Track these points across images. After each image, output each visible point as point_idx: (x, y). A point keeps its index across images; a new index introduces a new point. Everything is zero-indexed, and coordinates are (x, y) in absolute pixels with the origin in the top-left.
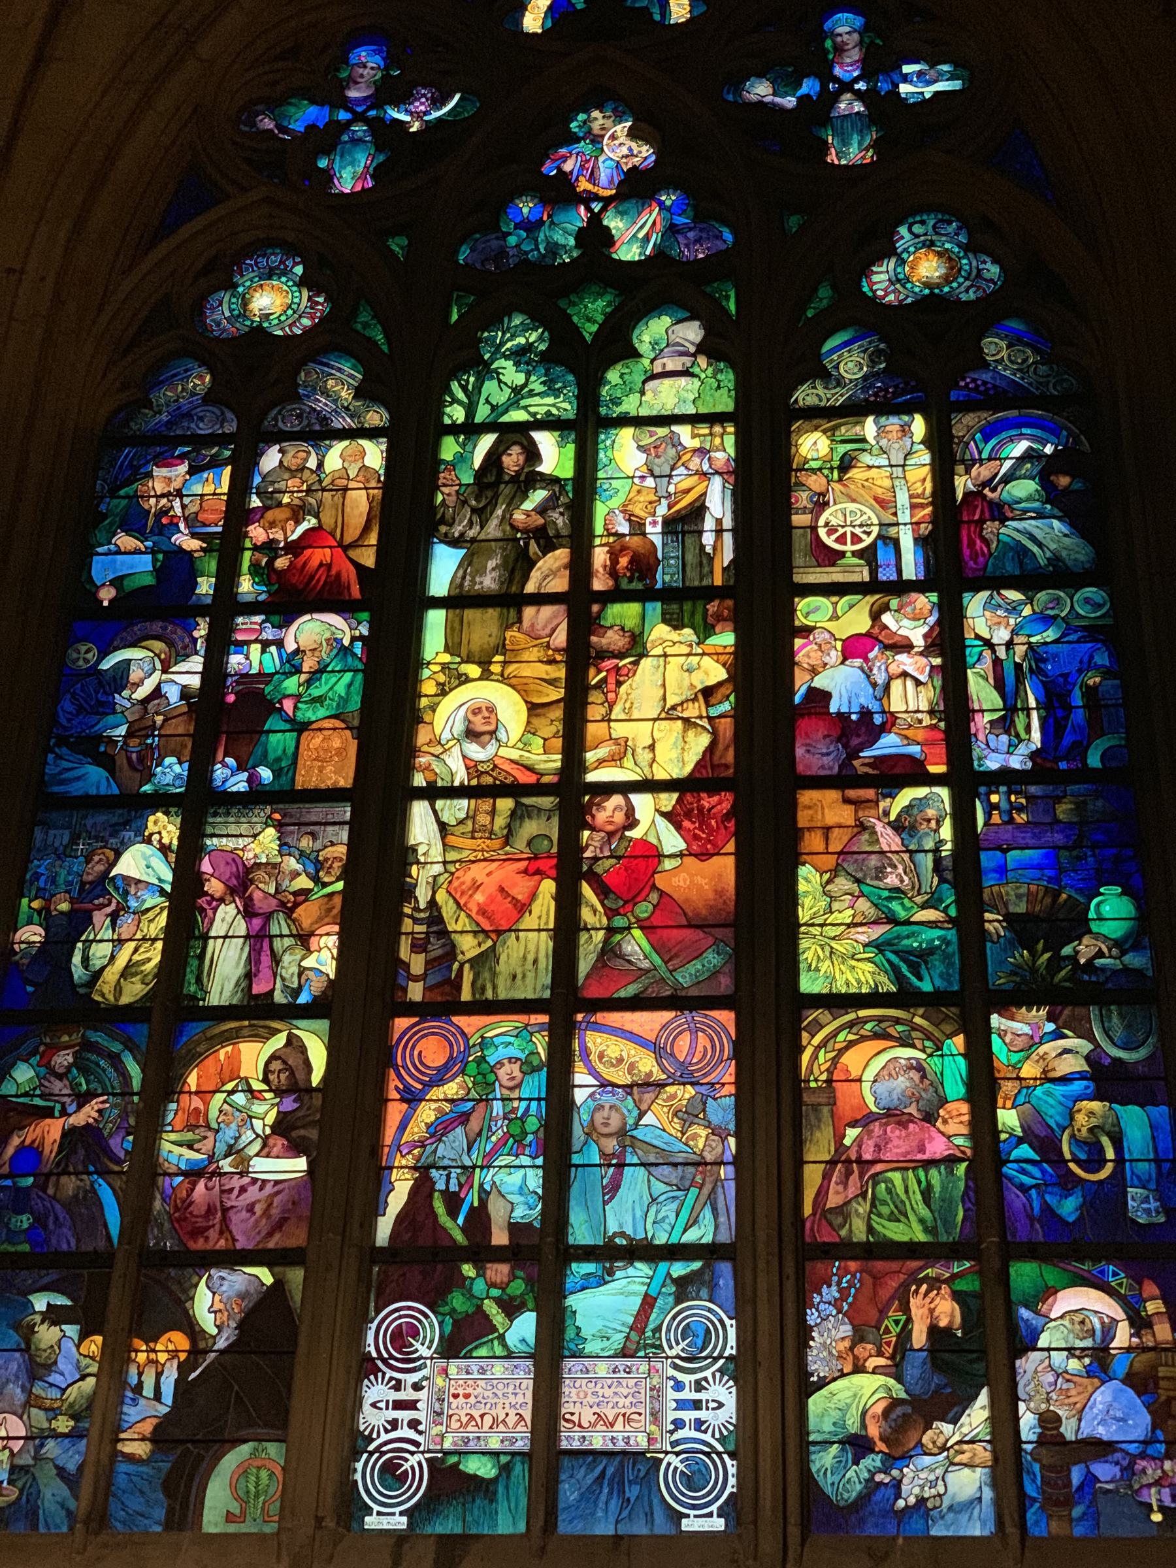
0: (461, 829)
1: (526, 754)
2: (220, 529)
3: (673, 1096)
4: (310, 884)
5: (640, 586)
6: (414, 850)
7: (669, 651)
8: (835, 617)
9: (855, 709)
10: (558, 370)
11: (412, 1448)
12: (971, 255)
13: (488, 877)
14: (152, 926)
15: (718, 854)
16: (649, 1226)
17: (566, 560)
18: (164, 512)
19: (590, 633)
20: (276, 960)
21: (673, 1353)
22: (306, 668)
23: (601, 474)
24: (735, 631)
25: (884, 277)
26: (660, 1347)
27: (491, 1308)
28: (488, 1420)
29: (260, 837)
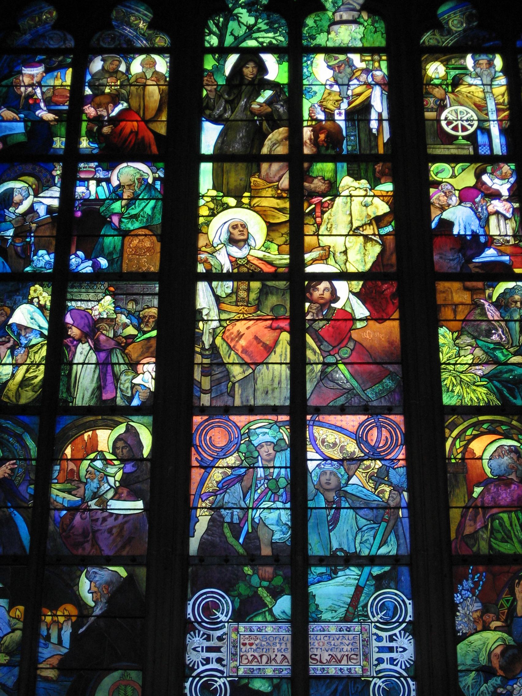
0: (229, 300)
1: (267, 254)
2: (66, 108)
3: (368, 467)
4: (135, 332)
5: (333, 153)
6: (200, 312)
7: (353, 193)
8: (453, 176)
9: (469, 233)
10: (275, 16)
11: (219, 675)
13: (248, 330)
14: (37, 356)
15: (389, 319)
16: (357, 545)
17: (286, 135)
18: (31, 96)
19: (303, 181)
20: (117, 378)
21: (375, 619)
22: (125, 197)
23: (305, 82)
24: (394, 182)
26: (367, 616)
27: (262, 592)
28: (265, 659)
29: (102, 302)
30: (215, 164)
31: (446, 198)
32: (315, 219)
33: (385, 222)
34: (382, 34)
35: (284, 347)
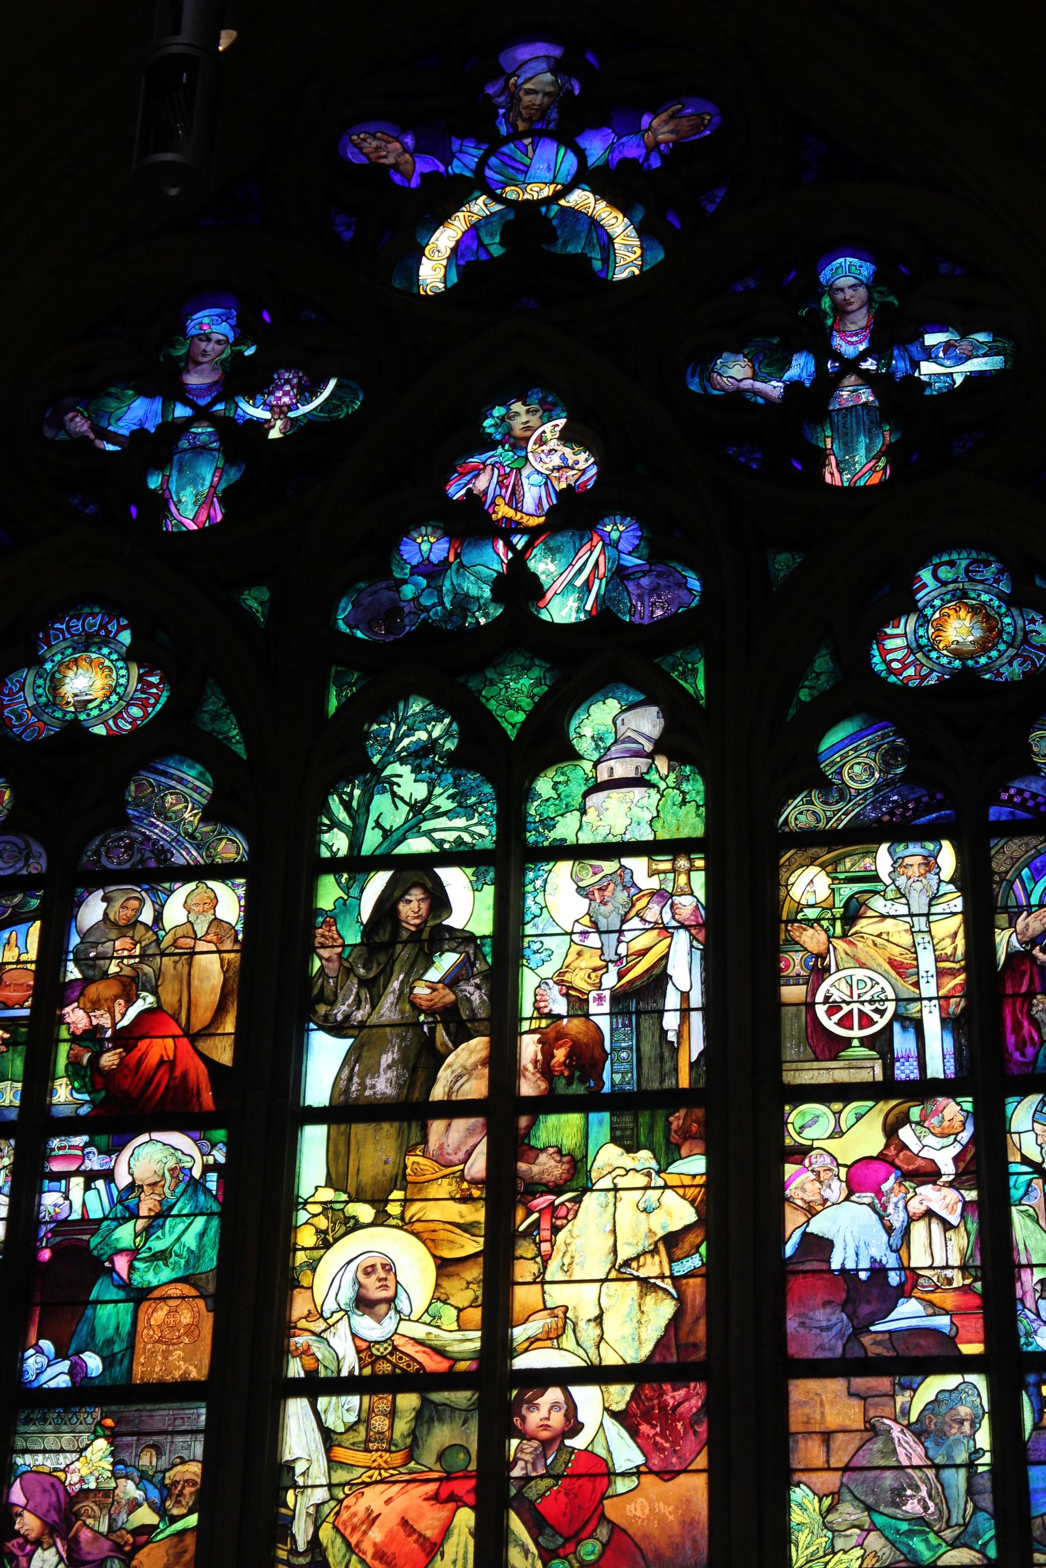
0: (351, 1438)
1: (435, 1331)
2: (26, 1012)
6: (289, 1467)
7: (621, 1183)
8: (838, 1133)
9: (865, 1264)
10: (471, 778)
12: (1015, 612)
15: (685, 1471)
17: (484, 1053)
22: (144, 1211)
23: (529, 929)
25: (900, 642)
29: (88, 1453)
30: (334, 1127)
31: (817, 1185)
32: (538, 1245)
33: (686, 1246)
34: (698, 806)
35: (463, 1540)
